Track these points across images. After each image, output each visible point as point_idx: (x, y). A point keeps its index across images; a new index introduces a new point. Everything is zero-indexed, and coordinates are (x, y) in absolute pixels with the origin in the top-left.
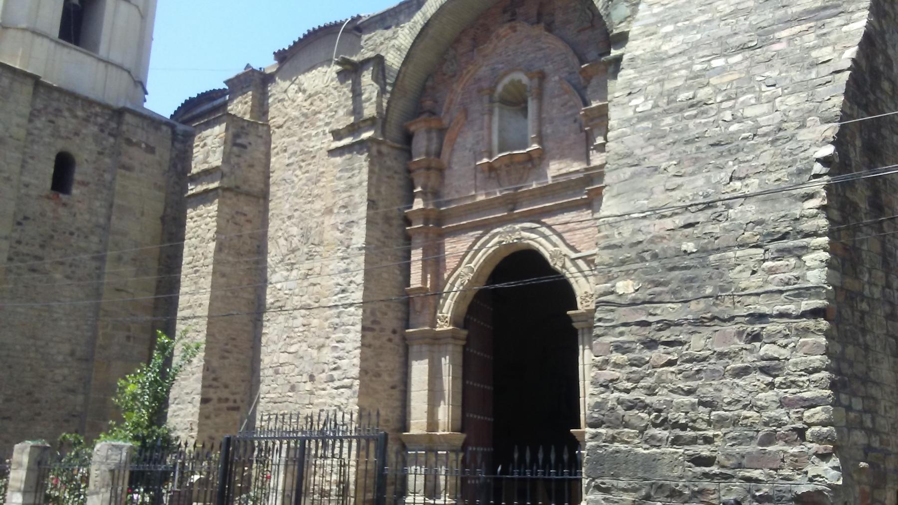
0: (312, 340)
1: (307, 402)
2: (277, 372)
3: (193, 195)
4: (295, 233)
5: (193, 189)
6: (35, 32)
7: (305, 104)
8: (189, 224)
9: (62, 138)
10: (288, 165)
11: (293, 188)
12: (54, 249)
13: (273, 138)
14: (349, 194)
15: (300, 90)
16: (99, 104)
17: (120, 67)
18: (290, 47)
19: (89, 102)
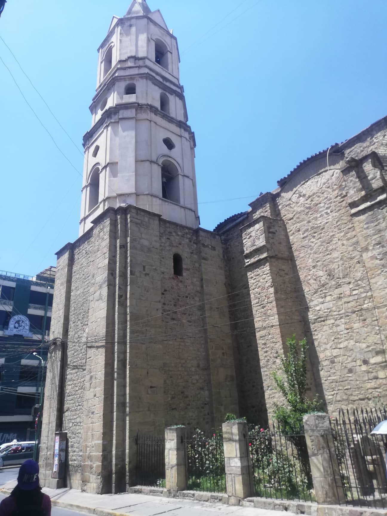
0: (358, 337)
1: (367, 378)
2: (333, 362)
3: (250, 265)
5: (248, 262)
6: (152, 195)
7: (307, 202)
8: (251, 282)
9: (173, 246)
10: (303, 238)
11: (311, 250)
13: (287, 226)
14: (380, 235)
15: (300, 196)
16: (187, 228)
17: (190, 209)
18: (288, 175)
19: (182, 227)
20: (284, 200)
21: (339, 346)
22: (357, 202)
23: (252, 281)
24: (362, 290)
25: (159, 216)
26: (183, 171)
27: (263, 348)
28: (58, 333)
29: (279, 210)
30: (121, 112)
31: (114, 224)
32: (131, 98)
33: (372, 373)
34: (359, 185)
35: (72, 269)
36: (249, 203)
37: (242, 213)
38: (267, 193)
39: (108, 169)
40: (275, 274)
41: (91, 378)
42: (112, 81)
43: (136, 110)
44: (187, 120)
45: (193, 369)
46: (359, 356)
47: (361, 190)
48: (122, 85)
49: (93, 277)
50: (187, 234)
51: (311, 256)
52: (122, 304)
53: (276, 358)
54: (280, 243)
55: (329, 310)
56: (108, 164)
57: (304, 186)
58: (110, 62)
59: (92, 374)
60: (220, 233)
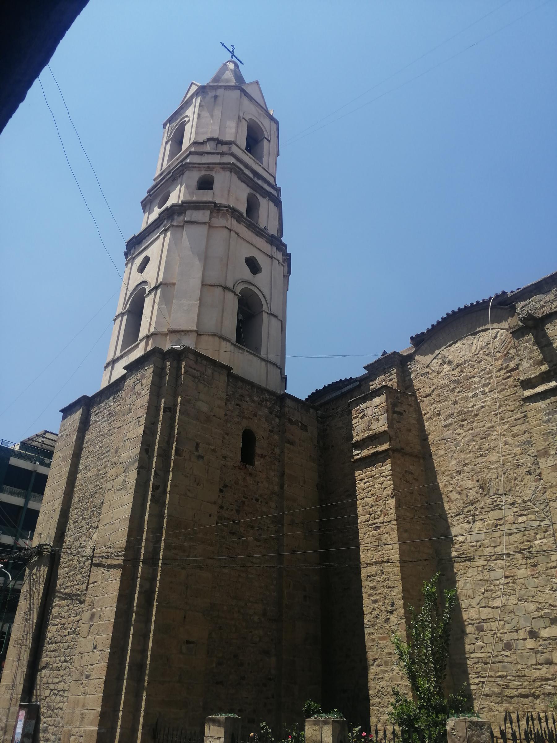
0: (522, 592)
1: (534, 662)
2: (480, 629)
3: (361, 458)
4: (470, 487)
5: (359, 454)
6: (221, 337)
7: (453, 373)
8: (360, 486)
10: (445, 426)
11: (456, 445)
12: (246, 514)
15: (444, 363)
16: (268, 392)
18: (428, 330)
19: (261, 390)
20: (419, 366)
21: (491, 604)
22: (533, 381)
23: (362, 485)
24: (533, 517)
25: (228, 369)
26: (269, 306)
27: (371, 595)
28: (48, 536)
29: (411, 381)
30: (188, 213)
31: (159, 374)
32: (206, 196)
33: (543, 653)
34: (538, 355)
35: (84, 436)
36: (365, 365)
37: (351, 378)
38: (395, 353)
39: (159, 291)
40: (400, 478)
41: (93, 616)
42: (181, 168)
43: (211, 213)
44: (281, 235)
45: (256, 618)
46: (523, 623)
47: (541, 363)
48: (194, 176)
49: (116, 452)
50: (266, 400)
51: (456, 455)
52: (158, 501)
53: (391, 612)
54: (409, 430)
55: (478, 544)
56: (161, 284)
57: (452, 349)
58: (180, 143)
59: (94, 610)
60: (316, 404)
